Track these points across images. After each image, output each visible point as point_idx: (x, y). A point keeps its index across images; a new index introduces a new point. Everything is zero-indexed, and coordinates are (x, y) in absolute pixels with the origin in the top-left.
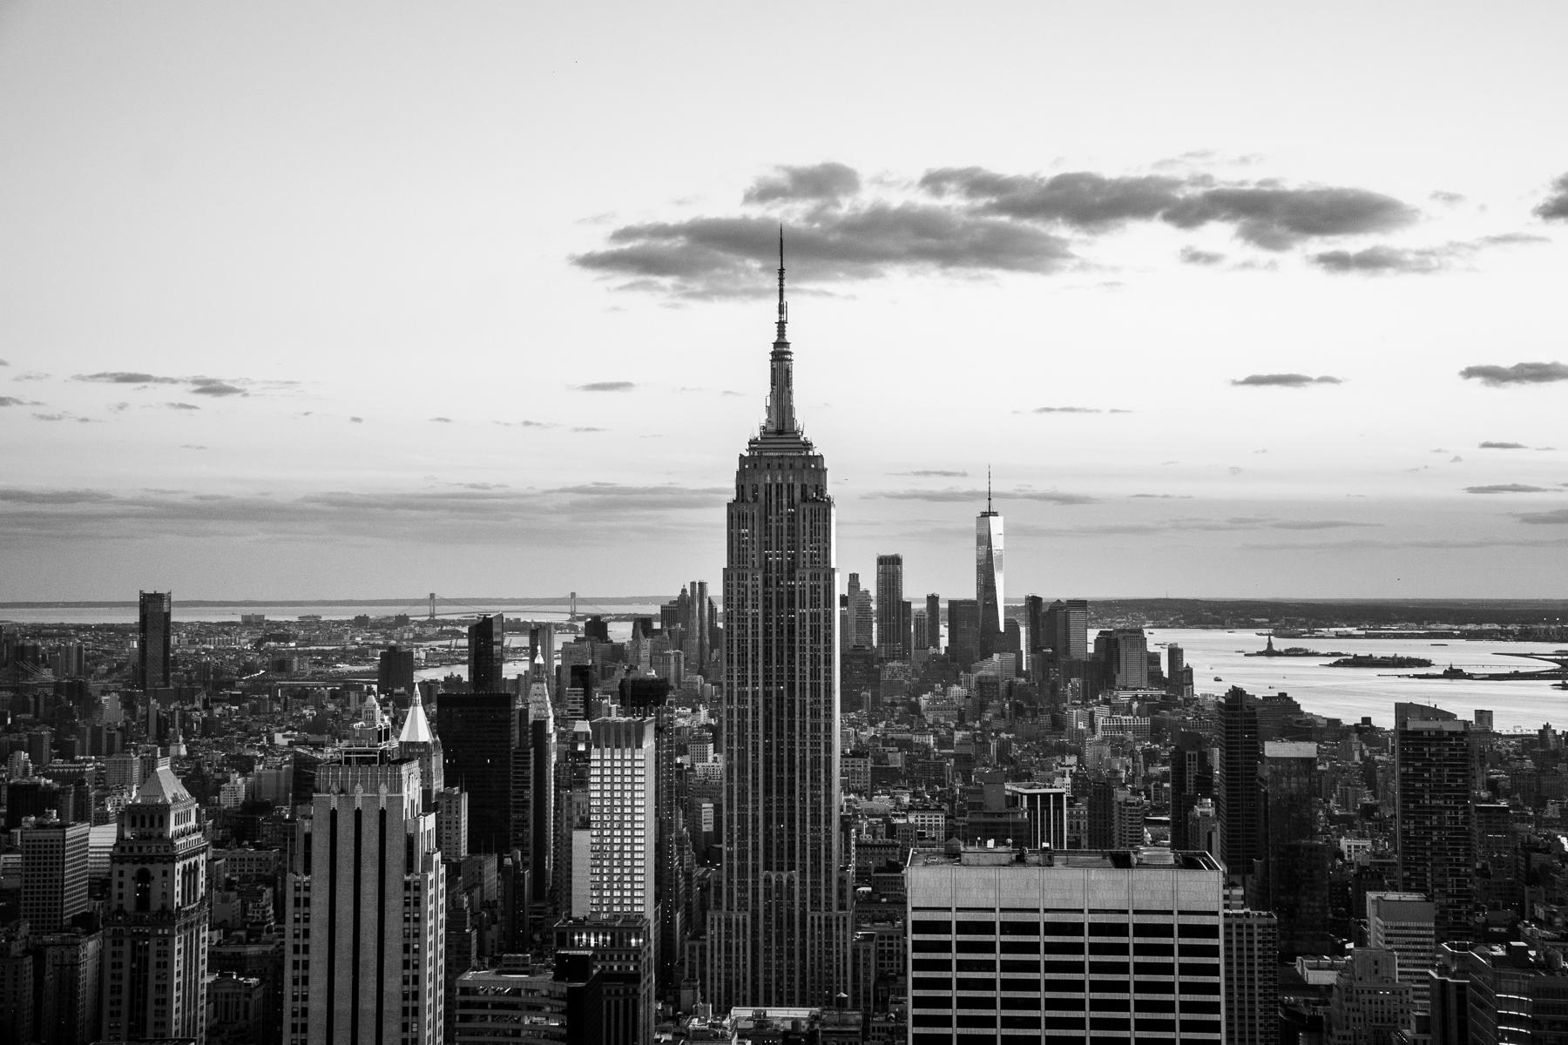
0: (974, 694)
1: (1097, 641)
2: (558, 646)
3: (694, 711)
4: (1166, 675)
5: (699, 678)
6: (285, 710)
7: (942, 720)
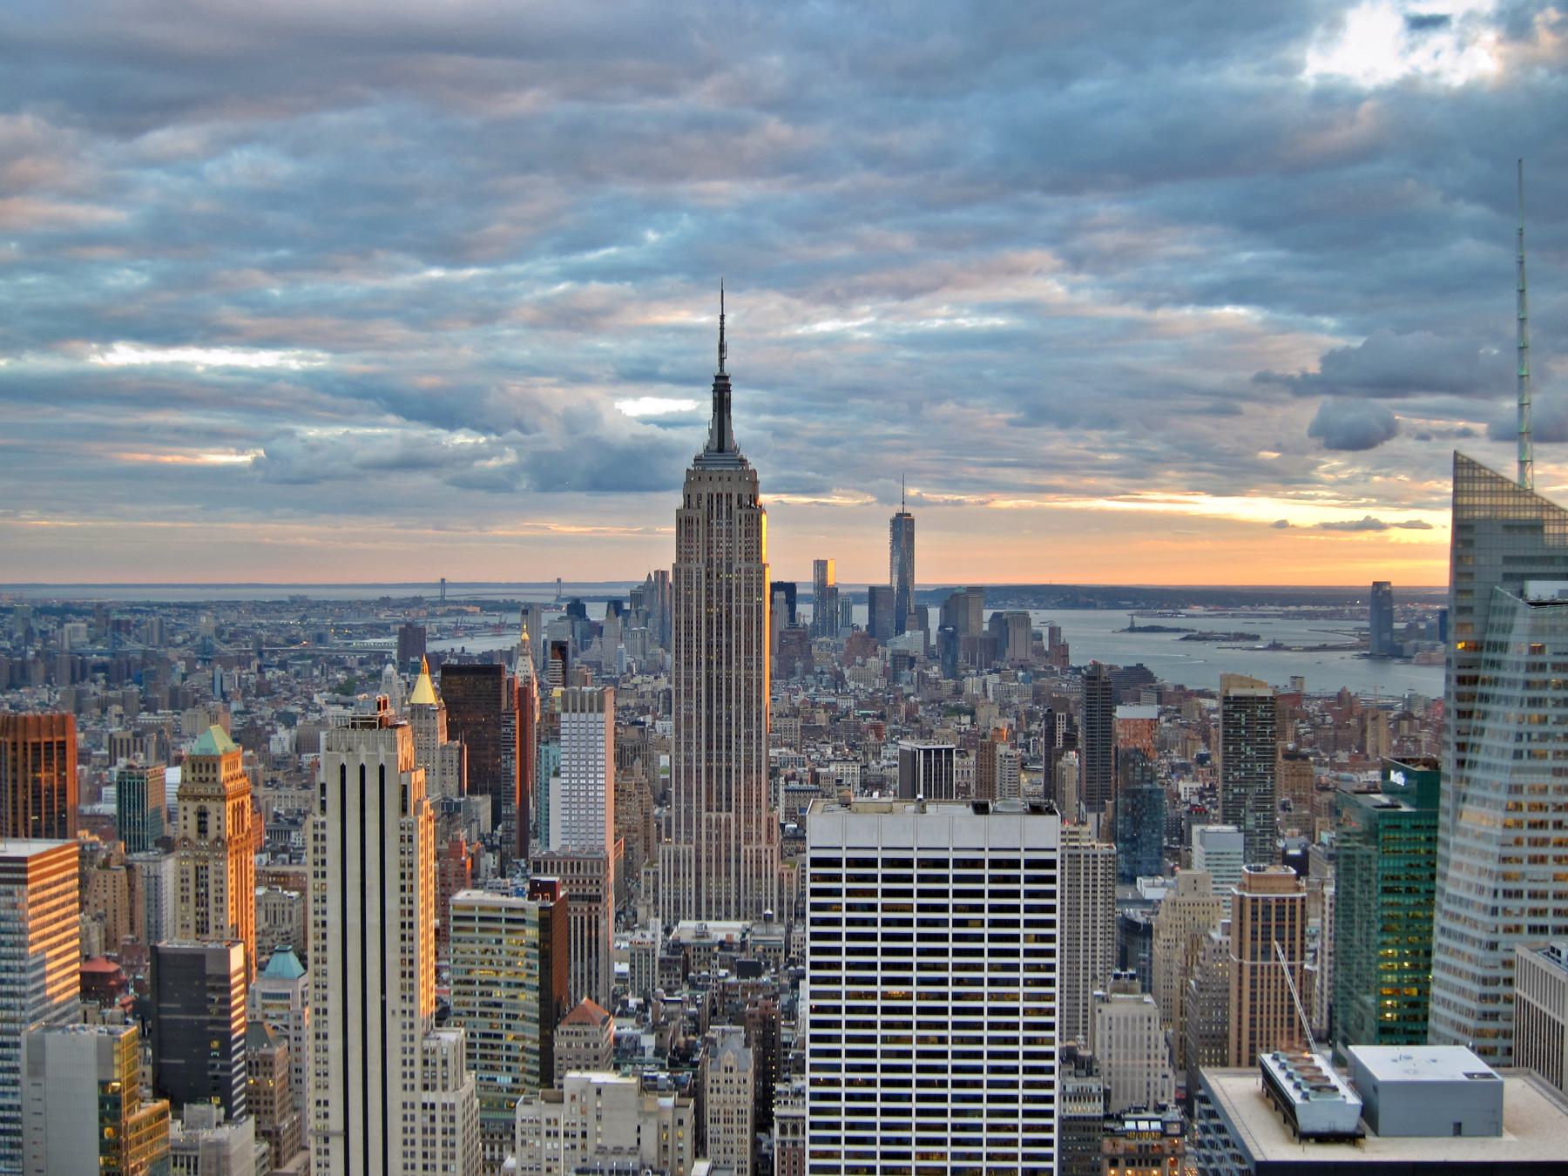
0: (888, 665)
1: (991, 621)
2: (545, 623)
3: (656, 678)
4: (1047, 648)
5: (660, 650)
6: (322, 674)
7: (862, 686)
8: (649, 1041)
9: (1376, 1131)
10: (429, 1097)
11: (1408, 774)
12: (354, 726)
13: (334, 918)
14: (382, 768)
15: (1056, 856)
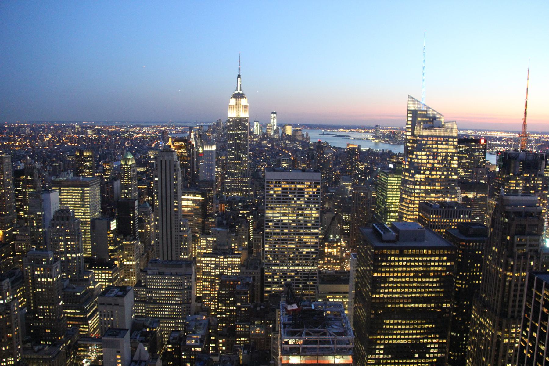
8: (225, 222)
9: (398, 241)
10: (181, 234)
11: (394, 165)
12: (164, 151)
13: (160, 194)
14: (170, 161)
15: (320, 181)
